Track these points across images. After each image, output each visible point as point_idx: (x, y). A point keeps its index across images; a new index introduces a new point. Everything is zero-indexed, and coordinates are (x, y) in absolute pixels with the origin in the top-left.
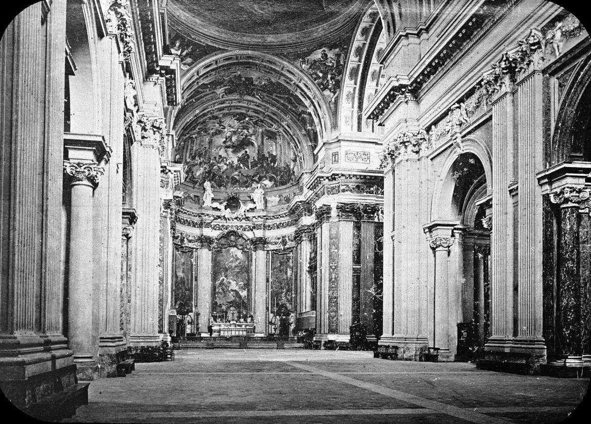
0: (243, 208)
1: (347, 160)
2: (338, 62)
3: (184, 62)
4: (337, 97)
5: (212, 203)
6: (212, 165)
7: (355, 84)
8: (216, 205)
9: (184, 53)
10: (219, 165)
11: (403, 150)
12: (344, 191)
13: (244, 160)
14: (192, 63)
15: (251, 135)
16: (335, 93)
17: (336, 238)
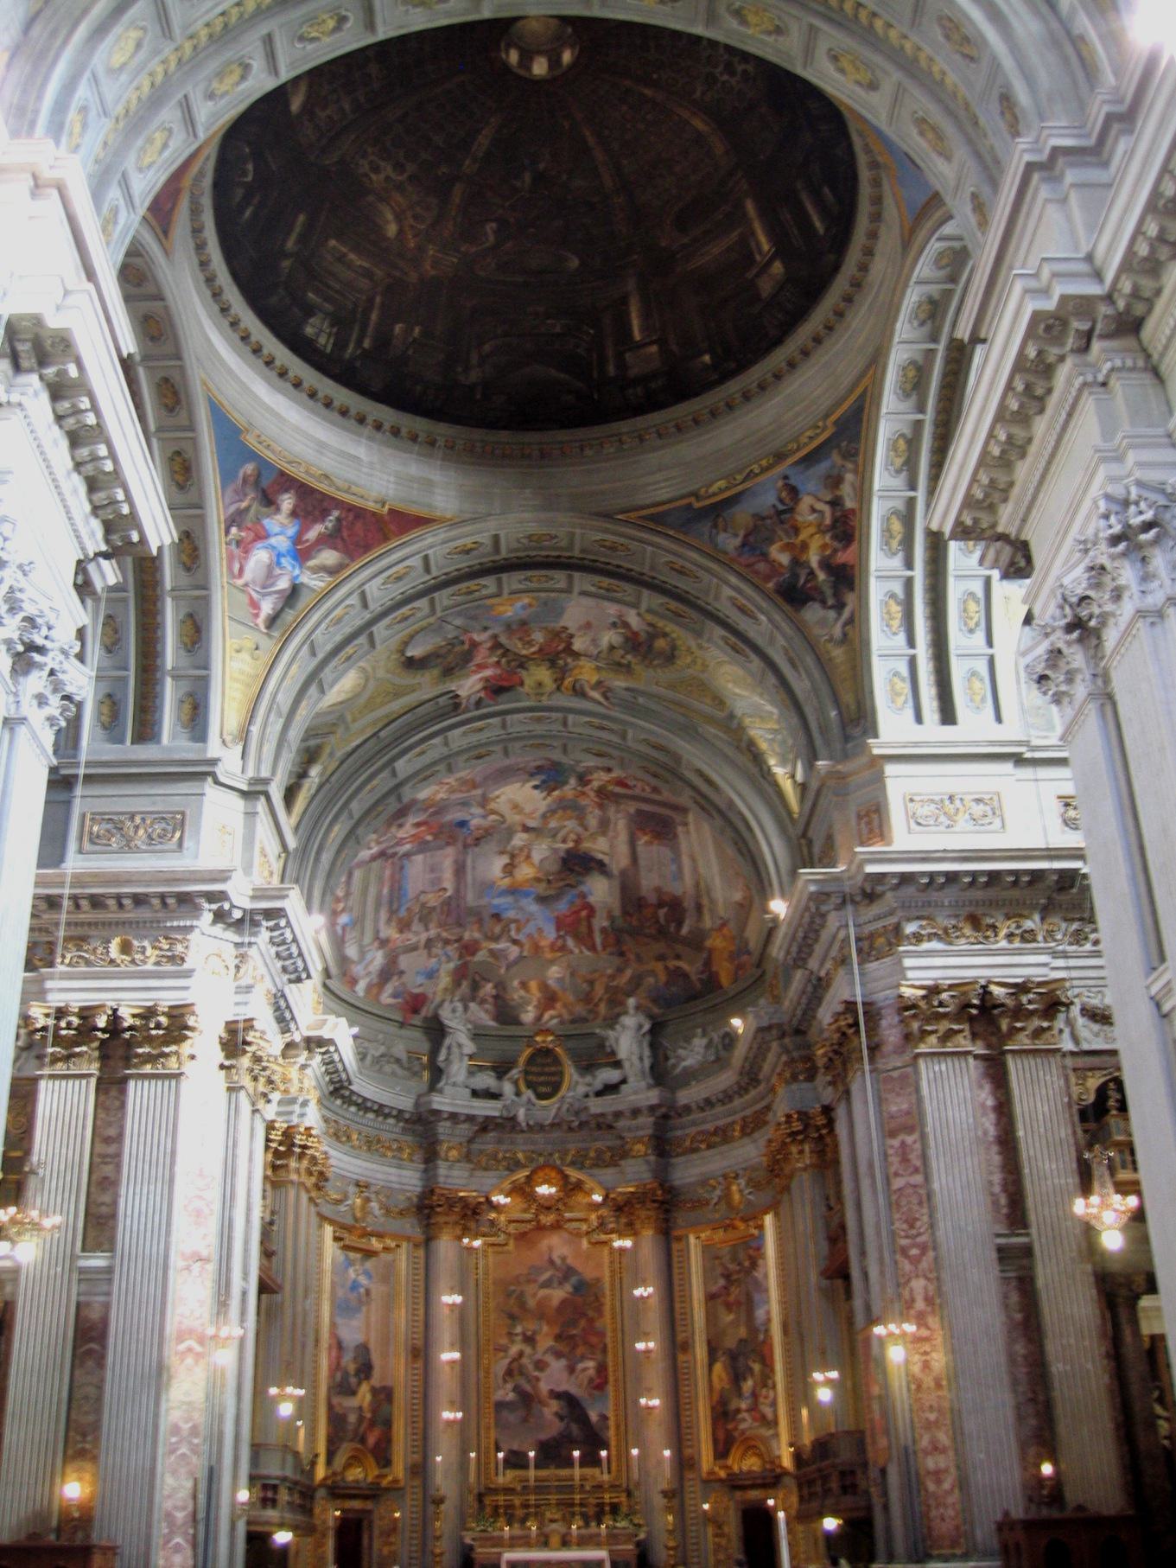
0: (575, 1084)
1: (913, 825)
2: (835, 503)
3: (311, 563)
4: (850, 621)
5: (471, 1072)
6: (469, 949)
7: (909, 564)
8: (486, 1080)
9: (312, 535)
10: (494, 946)
11: (1127, 574)
12: (918, 938)
13: (576, 925)
15: (593, 837)
16: (840, 606)
17: (910, 1129)
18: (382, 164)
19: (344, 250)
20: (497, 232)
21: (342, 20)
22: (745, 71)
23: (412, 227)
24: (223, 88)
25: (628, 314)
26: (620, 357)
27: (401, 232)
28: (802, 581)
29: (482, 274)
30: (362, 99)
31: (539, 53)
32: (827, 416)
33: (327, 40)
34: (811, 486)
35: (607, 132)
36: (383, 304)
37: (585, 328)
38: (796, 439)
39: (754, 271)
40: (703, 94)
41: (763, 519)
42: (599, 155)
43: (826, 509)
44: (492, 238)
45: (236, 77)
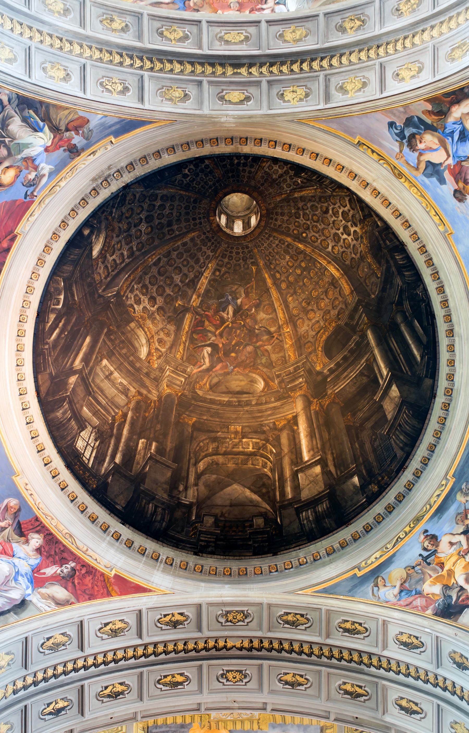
14: (67, 603)
18: (142, 297)
19: (112, 369)
20: (210, 355)
21: (126, 89)
22: (355, 231)
23: (157, 349)
24: (53, 75)
25: (299, 434)
26: (295, 475)
27: (149, 354)
28: (454, 598)
29: (200, 393)
30: (135, 249)
31: (238, 218)
32: (447, 474)
33: (115, 95)
34: (446, 529)
35: (278, 275)
36: (132, 418)
37: (269, 447)
38: (428, 502)
39: (379, 394)
40: (333, 247)
41: (413, 568)
42: (274, 293)
43: (462, 538)
44: (207, 360)
45: (62, 74)
